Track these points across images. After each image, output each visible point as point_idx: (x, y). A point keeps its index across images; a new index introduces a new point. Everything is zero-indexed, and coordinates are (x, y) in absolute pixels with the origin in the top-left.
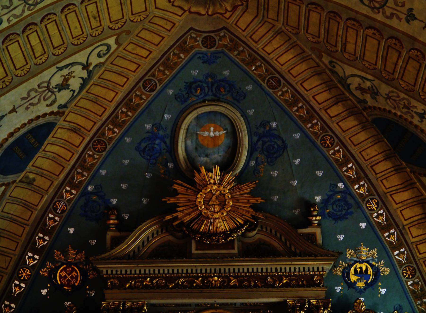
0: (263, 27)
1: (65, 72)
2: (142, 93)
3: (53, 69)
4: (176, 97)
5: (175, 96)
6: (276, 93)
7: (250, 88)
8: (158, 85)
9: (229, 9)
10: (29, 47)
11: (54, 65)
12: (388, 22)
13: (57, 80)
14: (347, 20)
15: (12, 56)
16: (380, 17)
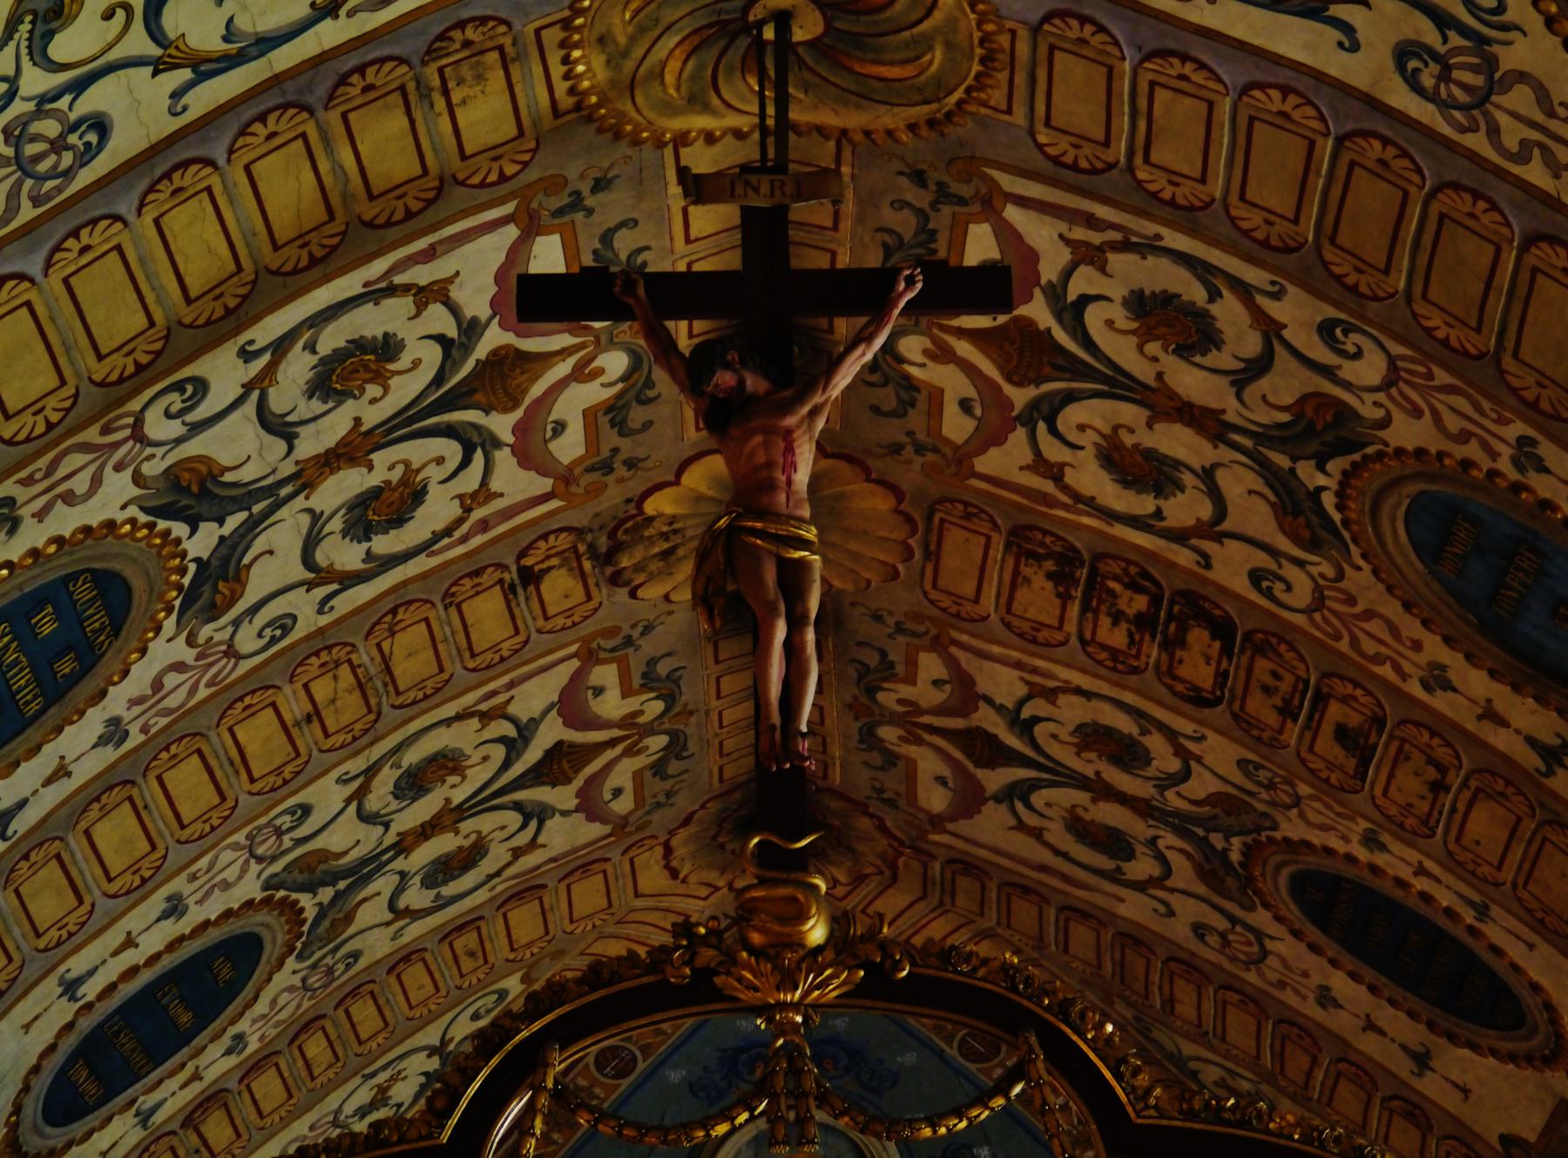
0: (942, 920)
1: (382, 1078)
2: (595, 1082)
3: (357, 1080)
4: (693, 1087)
5: (691, 1085)
6: (988, 1072)
7: (910, 1058)
8: (640, 1058)
9: (842, 878)
10: (300, 1063)
11: (355, 1074)
12: (1275, 992)
13: (364, 1095)
14: (1170, 959)
15: (257, 1097)
16: (1251, 977)
